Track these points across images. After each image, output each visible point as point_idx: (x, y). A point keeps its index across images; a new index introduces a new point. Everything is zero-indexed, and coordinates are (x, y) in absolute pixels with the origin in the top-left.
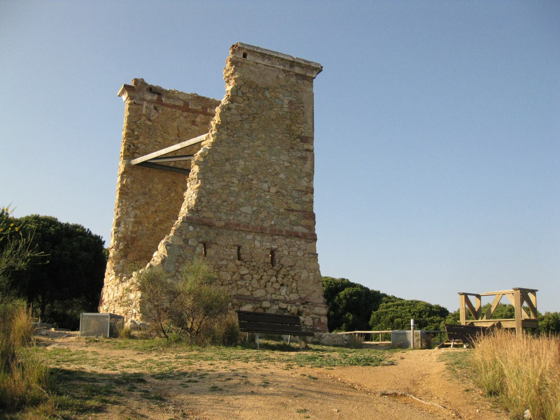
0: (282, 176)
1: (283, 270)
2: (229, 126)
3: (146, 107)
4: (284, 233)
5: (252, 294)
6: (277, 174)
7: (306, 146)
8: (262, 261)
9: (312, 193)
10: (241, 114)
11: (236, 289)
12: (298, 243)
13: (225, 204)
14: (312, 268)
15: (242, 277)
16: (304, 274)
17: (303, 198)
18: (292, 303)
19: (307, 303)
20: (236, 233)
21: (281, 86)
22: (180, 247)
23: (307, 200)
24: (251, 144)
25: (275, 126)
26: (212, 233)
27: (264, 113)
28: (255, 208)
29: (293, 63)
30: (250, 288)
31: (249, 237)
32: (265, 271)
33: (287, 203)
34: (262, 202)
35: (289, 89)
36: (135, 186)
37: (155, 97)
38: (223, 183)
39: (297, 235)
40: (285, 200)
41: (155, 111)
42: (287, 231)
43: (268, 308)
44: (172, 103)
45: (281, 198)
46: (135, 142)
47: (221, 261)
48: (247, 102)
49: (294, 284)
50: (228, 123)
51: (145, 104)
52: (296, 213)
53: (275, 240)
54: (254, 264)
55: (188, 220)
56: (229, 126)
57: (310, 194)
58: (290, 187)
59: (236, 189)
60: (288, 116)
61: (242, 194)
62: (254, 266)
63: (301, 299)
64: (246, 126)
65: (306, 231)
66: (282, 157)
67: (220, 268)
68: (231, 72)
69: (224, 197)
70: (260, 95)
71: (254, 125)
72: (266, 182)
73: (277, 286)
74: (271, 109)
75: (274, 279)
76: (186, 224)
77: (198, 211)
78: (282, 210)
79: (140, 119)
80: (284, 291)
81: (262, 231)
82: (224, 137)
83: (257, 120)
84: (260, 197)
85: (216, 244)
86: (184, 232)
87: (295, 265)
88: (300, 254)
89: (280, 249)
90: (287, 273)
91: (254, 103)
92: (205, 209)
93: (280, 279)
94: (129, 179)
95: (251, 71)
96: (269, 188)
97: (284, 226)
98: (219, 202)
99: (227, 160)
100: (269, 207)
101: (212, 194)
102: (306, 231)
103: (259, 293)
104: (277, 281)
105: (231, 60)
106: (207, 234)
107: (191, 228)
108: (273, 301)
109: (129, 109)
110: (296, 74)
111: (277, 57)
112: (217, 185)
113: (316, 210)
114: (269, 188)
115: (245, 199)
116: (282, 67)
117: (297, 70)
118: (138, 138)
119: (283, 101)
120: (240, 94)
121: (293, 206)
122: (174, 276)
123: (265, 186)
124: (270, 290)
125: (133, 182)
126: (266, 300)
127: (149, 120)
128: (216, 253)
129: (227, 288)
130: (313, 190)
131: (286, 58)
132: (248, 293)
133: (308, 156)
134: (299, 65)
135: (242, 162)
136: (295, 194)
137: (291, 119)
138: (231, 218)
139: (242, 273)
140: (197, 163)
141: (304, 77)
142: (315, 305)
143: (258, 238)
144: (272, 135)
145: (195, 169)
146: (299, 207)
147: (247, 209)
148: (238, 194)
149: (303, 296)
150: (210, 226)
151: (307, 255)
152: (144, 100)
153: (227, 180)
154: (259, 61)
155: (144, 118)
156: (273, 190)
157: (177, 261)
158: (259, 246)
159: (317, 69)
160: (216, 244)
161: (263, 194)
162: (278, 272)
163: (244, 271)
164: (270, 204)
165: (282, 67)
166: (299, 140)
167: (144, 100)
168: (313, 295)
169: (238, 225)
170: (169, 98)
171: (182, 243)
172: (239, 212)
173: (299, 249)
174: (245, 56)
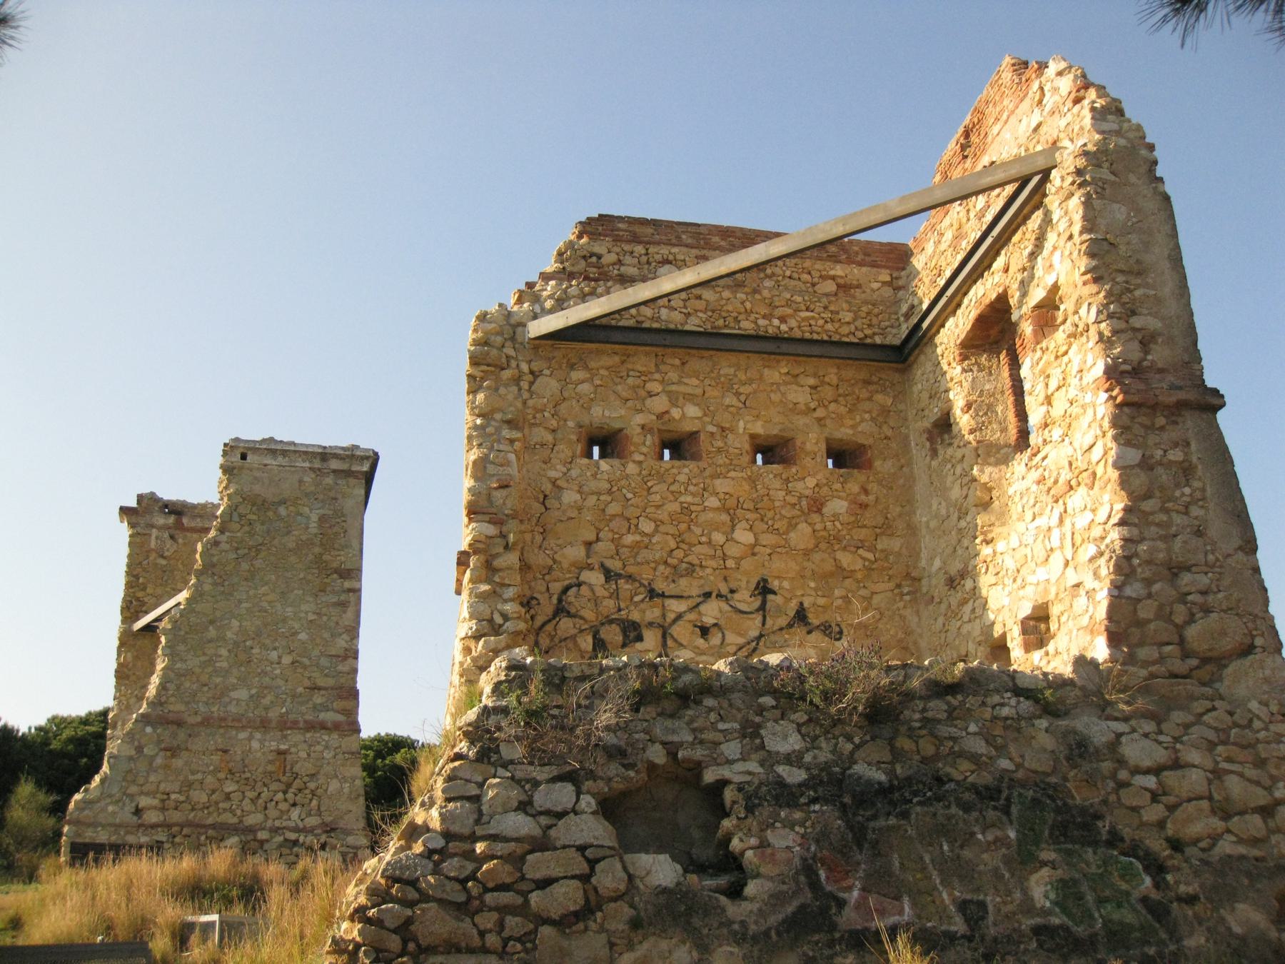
0: (303, 636)
1: (298, 781)
2: (215, 570)
3: (157, 538)
4: (301, 725)
5: (241, 822)
6: (296, 633)
7: (347, 584)
8: (260, 770)
9: (356, 658)
10: (237, 549)
11: (215, 814)
12: (326, 738)
13: (206, 689)
14: (348, 774)
15: (228, 797)
16: (334, 786)
17: (340, 668)
18: (311, 831)
19: (333, 830)
20: (222, 731)
21: (307, 495)
22: (131, 758)
23: (346, 669)
24: (252, 592)
25: (293, 559)
26: (182, 735)
27: (276, 542)
28: (254, 691)
29: (325, 455)
30: (239, 812)
31: (242, 735)
32: (265, 785)
33: (309, 678)
34: (267, 680)
35: (321, 497)
36: (139, 664)
37: (171, 519)
38: (203, 659)
39: (323, 727)
40: (307, 674)
41: (169, 543)
42: (306, 722)
43: (267, 841)
44: (200, 525)
45: (299, 670)
46: (140, 594)
47: (193, 774)
48: (246, 528)
49: (314, 802)
50: (214, 566)
51: (154, 532)
52: (322, 692)
53: (285, 737)
54: (248, 775)
55: (145, 719)
56: (215, 570)
57: (350, 660)
58: (316, 652)
59: (225, 664)
60: (317, 541)
61: (235, 671)
62: (247, 779)
63: (324, 824)
64: (245, 566)
65: (340, 718)
66: (304, 607)
67: (190, 785)
68: (224, 485)
69: (204, 678)
70: (270, 514)
71: (258, 563)
72: (275, 649)
73: (283, 806)
74: (289, 533)
75: (280, 796)
76: (140, 725)
77: (161, 704)
78: (300, 690)
79: (148, 557)
80: (295, 813)
81: (264, 725)
82: (207, 587)
83: (263, 554)
84: (265, 673)
85: (187, 749)
86: (137, 736)
87: (318, 772)
88: (328, 755)
89: (293, 750)
90: (302, 786)
91: (258, 527)
92: (172, 699)
93: (290, 796)
94: (129, 655)
95: (256, 478)
96: (280, 657)
97: (304, 714)
98: (194, 687)
99: (212, 622)
100: (280, 687)
101: (184, 675)
102: (340, 718)
103: (251, 820)
104: (286, 800)
105: (222, 467)
106: (174, 736)
107: (149, 730)
108: (275, 830)
109: (130, 544)
110: (334, 471)
111: (295, 452)
112: (193, 662)
113: (362, 683)
114: (280, 657)
115: (239, 679)
116: (307, 465)
117: (335, 464)
118: (144, 589)
119: (308, 518)
120: (235, 518)
121: (321, 682)
122: (118, 802)
123: (274, 655)
124: (272, 813)
125: (136, 658)
126: (264, 829)
127: (162, 557)
128: (186, 763)
129: (200, 814)
130: (356, 652)
131: (310, 450)
132: (235, 820)
133: (350, 599)
134: (336, 456)
135: (235, 623)
136: (324, 662)
137: (322, 545)
138: (215, 709)
139: (227, 790)
140: (165, 632)
141: (348, 474)
142: (348, 832)
143: (258, 735)
144: (289, 575)
145: (163, 639)
146: (330, 682)
147: (242, 694)
148: (227, 672)
149: (328, 819)
150: (179, 724)
151: (340, 756)
152: (152, 526)
153: (210, 652)
154: (268, 461)
155: (153, 556)
156: (287, 660)
157: (124, 780)
158: (259, 747)
159: (367, 458)
160: (187, 749)
161: (269, 668)
162: (289, 785)
163: (230, 787)
164: (280, 682)
165: (307, 465)
166: (335, 576)
167: (152, 526)
168: (346, 817)
169: (224, 719)
170: (194, 517)
171: (133, 752)
172: (227, 699)
173: (327, 747)
174: (244, 457)
